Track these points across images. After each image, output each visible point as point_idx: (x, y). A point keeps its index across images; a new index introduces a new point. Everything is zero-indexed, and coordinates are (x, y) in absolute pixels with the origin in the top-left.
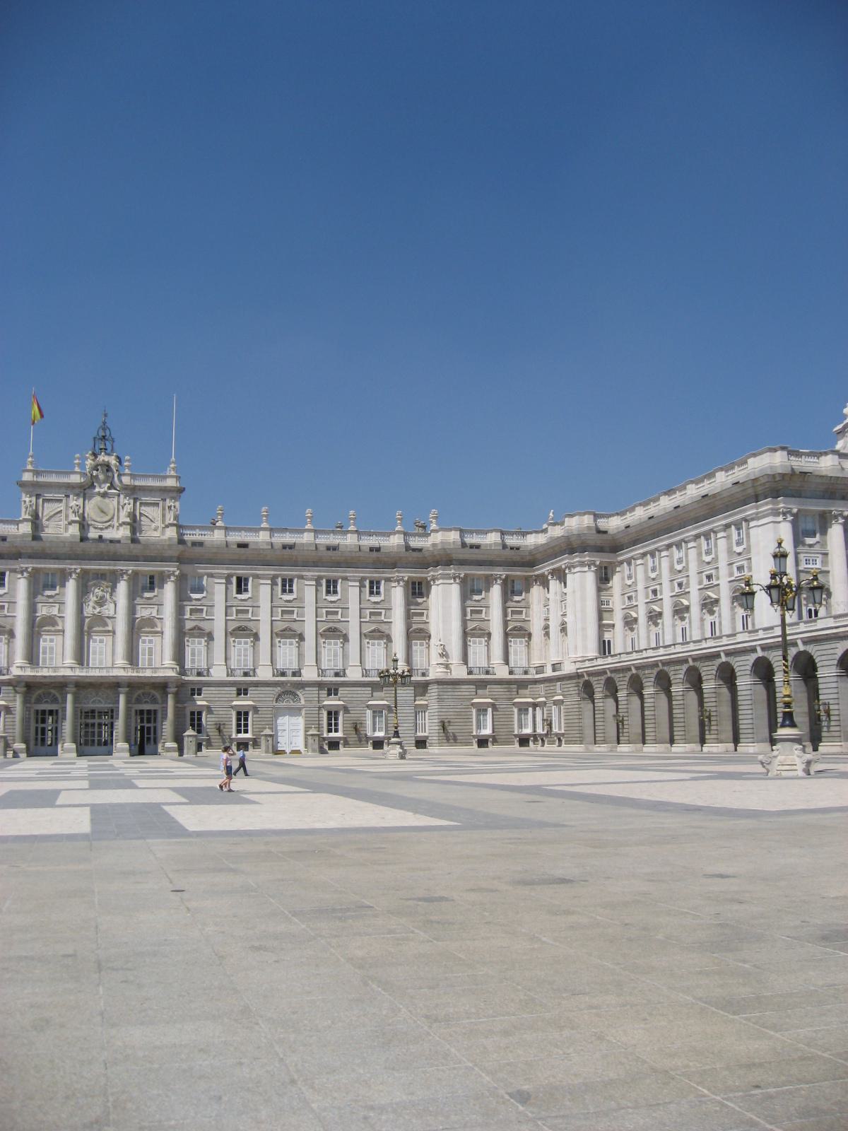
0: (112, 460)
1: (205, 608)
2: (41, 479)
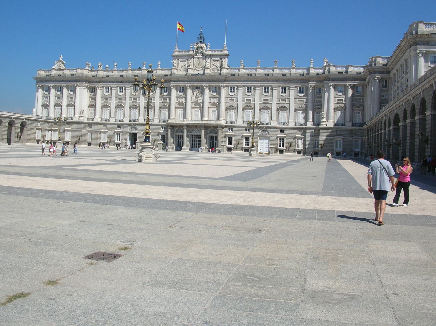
0: (203, 45)
1: (235, 99)
2: (180, 54)
